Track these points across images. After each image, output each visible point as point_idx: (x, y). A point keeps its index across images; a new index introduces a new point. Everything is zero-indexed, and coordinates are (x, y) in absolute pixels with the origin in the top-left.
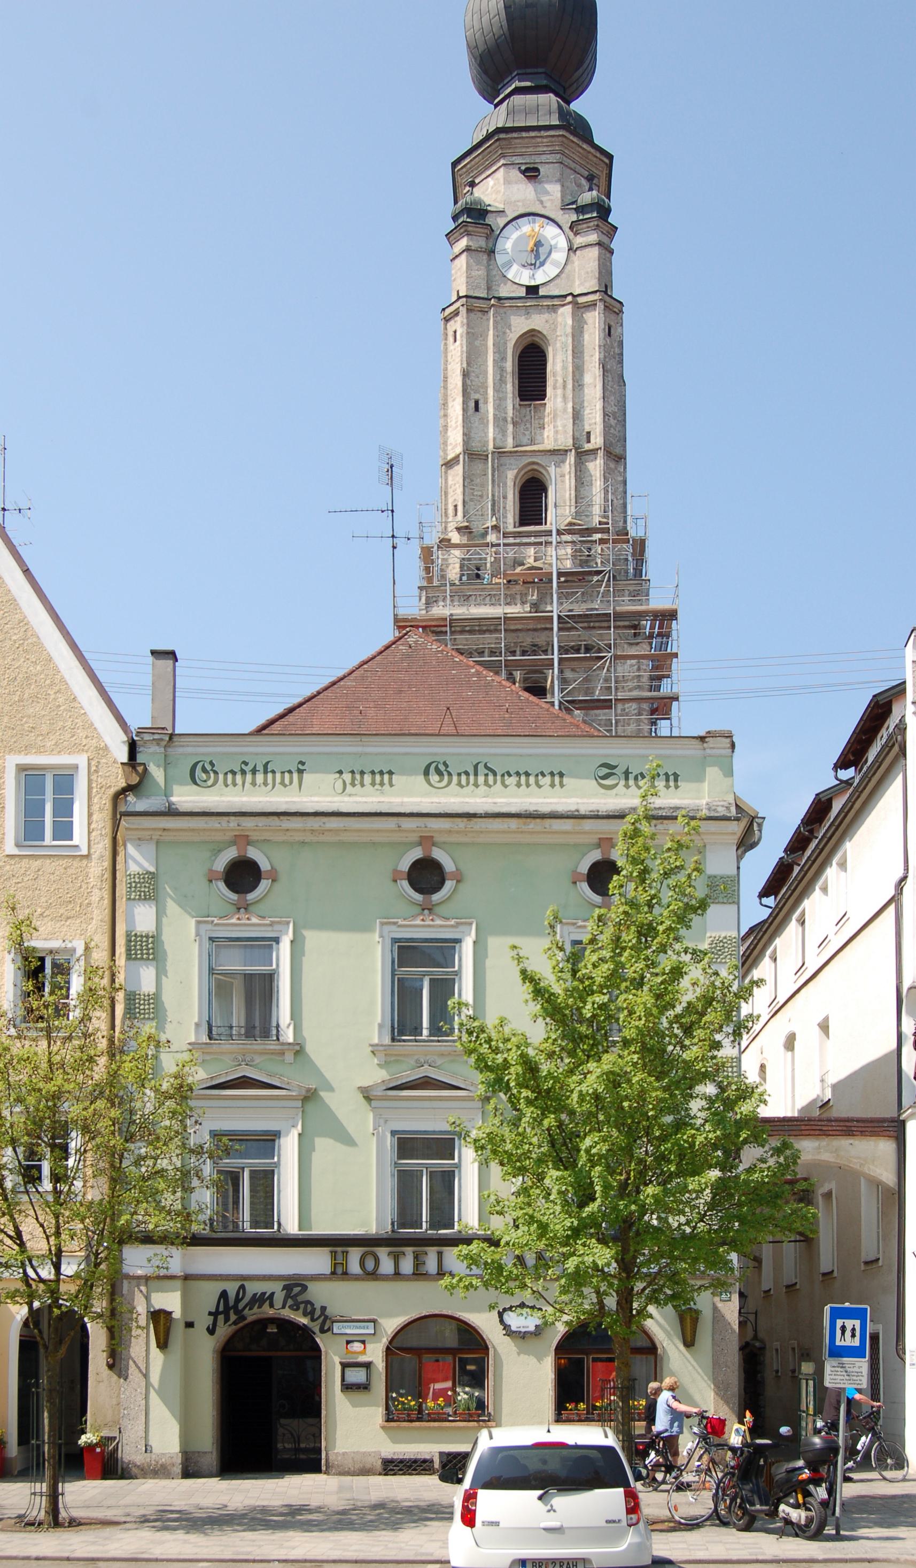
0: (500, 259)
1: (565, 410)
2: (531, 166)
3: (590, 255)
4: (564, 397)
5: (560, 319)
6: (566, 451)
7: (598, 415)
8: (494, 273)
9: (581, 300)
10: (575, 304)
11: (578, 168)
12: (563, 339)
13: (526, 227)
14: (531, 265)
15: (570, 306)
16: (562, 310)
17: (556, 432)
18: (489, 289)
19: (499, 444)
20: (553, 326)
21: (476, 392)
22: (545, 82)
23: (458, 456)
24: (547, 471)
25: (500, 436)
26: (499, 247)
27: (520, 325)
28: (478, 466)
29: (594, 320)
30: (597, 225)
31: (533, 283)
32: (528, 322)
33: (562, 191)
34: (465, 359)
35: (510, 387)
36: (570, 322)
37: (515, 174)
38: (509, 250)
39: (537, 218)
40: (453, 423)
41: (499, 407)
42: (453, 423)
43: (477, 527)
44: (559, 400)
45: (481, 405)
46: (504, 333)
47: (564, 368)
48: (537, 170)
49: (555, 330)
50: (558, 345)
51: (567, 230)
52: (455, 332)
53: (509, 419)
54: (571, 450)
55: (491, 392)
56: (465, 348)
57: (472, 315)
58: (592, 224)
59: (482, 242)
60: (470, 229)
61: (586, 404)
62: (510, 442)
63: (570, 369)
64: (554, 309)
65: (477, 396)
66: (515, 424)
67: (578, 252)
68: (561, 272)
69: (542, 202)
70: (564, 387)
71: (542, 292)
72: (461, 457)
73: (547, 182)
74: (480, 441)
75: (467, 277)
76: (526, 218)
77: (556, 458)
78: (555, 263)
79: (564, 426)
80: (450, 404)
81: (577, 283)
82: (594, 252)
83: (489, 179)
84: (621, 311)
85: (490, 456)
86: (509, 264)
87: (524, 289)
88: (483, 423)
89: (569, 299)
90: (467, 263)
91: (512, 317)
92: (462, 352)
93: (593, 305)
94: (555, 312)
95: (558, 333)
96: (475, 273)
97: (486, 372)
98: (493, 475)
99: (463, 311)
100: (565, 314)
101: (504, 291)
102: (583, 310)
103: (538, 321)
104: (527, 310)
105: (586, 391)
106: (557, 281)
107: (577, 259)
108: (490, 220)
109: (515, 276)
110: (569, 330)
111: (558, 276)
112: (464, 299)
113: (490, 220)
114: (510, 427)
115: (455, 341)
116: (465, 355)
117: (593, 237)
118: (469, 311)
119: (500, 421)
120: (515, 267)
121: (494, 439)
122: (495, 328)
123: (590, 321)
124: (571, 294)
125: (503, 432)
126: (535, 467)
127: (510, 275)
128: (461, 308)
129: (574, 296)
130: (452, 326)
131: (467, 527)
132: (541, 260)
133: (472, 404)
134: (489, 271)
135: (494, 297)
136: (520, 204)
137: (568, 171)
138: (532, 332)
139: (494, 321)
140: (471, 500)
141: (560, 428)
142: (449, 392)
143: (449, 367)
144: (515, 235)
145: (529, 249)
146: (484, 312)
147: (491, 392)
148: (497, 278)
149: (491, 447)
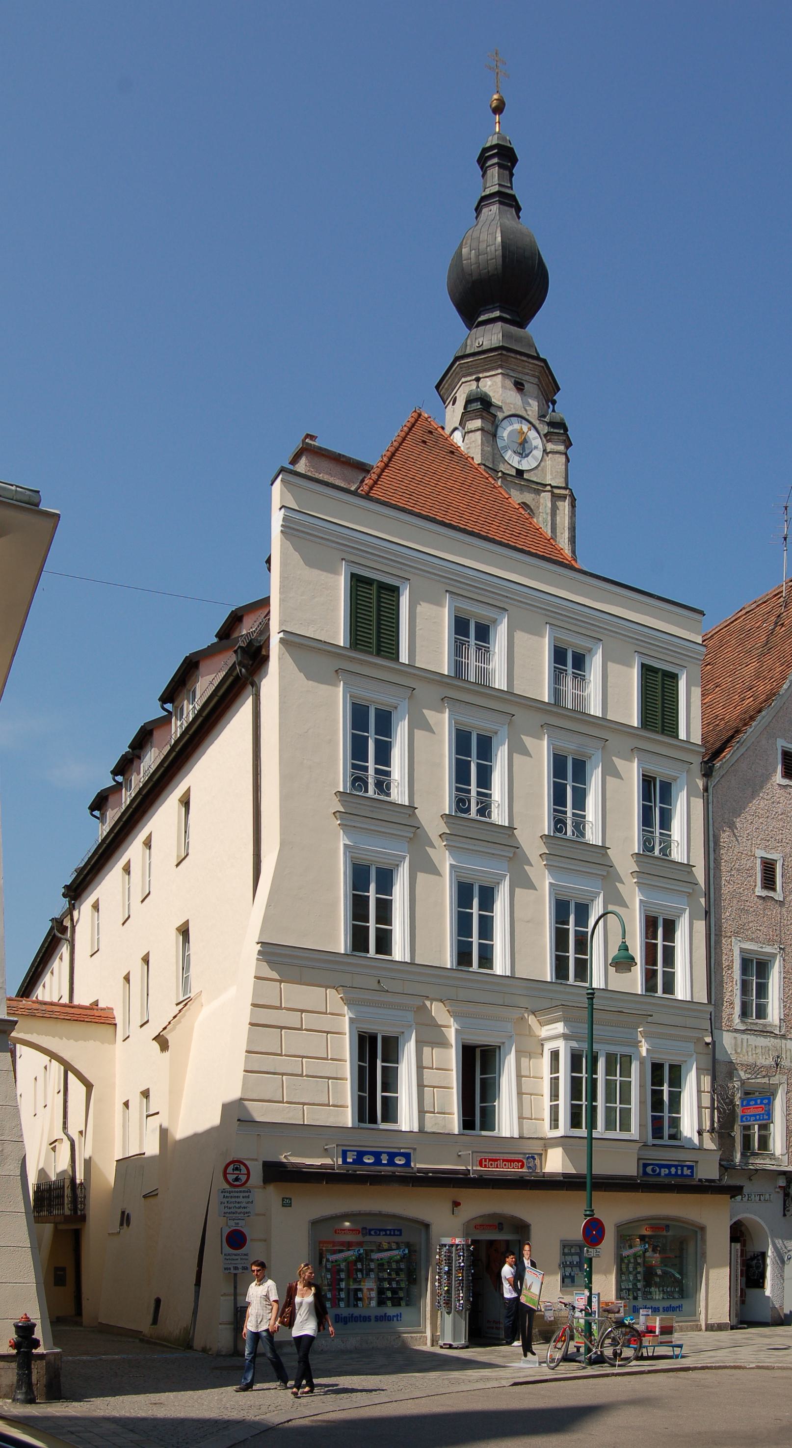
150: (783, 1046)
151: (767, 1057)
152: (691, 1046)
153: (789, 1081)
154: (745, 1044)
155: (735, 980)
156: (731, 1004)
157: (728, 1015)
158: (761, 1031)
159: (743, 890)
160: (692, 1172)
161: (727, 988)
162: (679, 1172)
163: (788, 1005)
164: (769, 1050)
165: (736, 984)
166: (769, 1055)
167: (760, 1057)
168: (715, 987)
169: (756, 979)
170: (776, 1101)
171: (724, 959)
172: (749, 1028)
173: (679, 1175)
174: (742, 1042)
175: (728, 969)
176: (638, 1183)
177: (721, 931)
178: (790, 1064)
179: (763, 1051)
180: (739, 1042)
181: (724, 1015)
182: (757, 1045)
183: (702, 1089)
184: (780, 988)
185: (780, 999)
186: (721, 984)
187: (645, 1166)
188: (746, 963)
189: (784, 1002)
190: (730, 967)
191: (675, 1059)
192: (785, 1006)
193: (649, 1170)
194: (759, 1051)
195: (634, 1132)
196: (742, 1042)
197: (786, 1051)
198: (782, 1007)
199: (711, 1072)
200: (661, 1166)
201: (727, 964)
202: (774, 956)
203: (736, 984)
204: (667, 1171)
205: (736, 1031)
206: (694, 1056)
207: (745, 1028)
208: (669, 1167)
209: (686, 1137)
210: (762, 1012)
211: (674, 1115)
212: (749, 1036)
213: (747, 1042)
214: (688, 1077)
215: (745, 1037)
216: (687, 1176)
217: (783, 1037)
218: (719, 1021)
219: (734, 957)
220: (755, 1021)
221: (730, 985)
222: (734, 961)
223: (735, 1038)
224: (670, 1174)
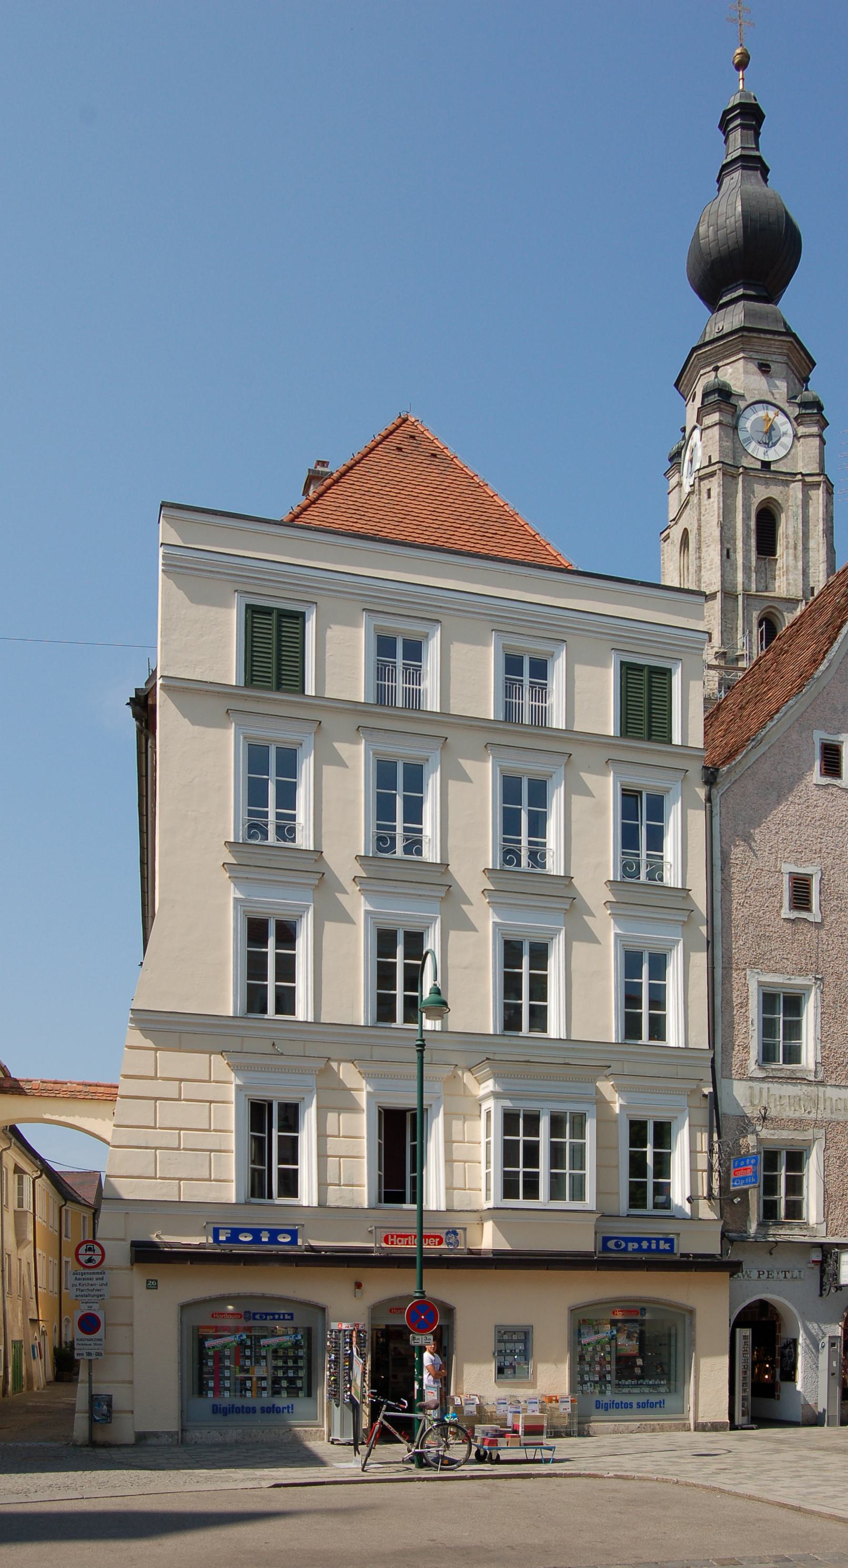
0: (742, 435)
1: (796, 567)
2: (765, 362)
3: (813, 443)
4: (795, 557)
5: (791, 492)
6: (798, 601)
7: (821, 574)
8: (737, 446)
9: (808, 479)
10: (803, 481)
11: (795, 371)
12: (794, 509)
13: (761, 412)
14: (765, 443)
15: (801, 483)
16: (792, 485)
17: (789, 584)
18: (734, 458)
19: (746, 588)
20: (786, 497)
21: (728, 542)
22: (765, 294)
23: (716, 593)
24: (783, 615)
25: (746, 581)
26: (741, 423)
27: (761, 492)
28: (730, 603)
29: (818, 496)
30: (819, 420)
31: (766, 459)
32: (768, 490)
33: (788, 387)
34: (721, 514)
35: (753, 542)
36: (800, 496)
37: (753, 367)
38: (749, 429)
39: (770, 407)
40: (707, 565)
41: (746, 557)
42: (707, 565)
43: (731, 655)
44: (791, 558)
45: (731, 554)
46: (750, 497)
47: (795, 533)
48: (769, 366)
49: (787, 500)
50: (790, 513)
51: (792, 420)
52: (709, 490)
53: (753, 568)
54: (802, 600)
55: (739, 544)
56: (721, 505)
57: (725, 478)
58: (814, 418)
59: (728, 419)
60: (722, 406)
61: (811, 564)
62: (753, 586)
63: (801, 534)
64: (786, 483)
65: (729, 546)
66: (756, 573)
67: (801, 440)
68: (788, 454)
69: (773, 394)
70: (795, 548)
71: (773, 468)
72: (719, 595)
73: (778, 378)
74: (730, 583)
75: (720, 446)
76: (761, 405)
77: (789, 605)
78: (784, 446)
79: (795, 580)
80: (704, 549)
81: (800, 464)
82: (816, 441)
83: (728, 367)
84: (833, 493)
85: (740, 598)
86: (749, 440)
87: (760, 463)
88: (732, 569)
89: (799, 477)
90: (720, 434)
91: (755, 485)
92: (719, 508)
93: (816, 485)
94: (788, 486)
95: (790, 504)
96: (725, 444)
97: (735, 527)
98: (743, 613)
99: (719, 474)
100: (796, 489)
101: (746, 462)
102: (808, 488)
103: (774, 492)
104: (767, 482)
105: (811, 554)
106: (785, 460)
107: (800, 446)
108: (733, 401)
109: (754, 450)
110: (800, 503)
111: (785, 456)
112: (721, 465)
113: (733, 401)
114: (754, 575)
115: (709, 497)
116: (721, 511)
117: (815, 430)
118: (724, 474)
119: (747, 569)
120: (753, 444)
121: (743, 583)
122: (743, 492)
123: (814, 497)
124: (801, 473)
125: (749, 578)
126: (772, 610)
127: (749, 451)
128: (718, 471)
129: (803, 475)
130: (705, 485)
131: (724, 653)
132: (774, 441)
133: (725, 552)
134: (734, 443)
135: (742, 466)
136: (756, 392)
137: (790, 372)
138: (770, 500)
139: (743, 486)
140: (725, 631)
141: (791, 581)
142: (703, 539)
143: (703, 518)
144: (753, 417)
145: (765, 430)
146: (734, 477)
147: (739, 544)
148: (739, 450)
149: (740, 588)
150: (821, 1095)
151: (797, 1108)
152: (684, 1100)
153: (829, 1136)
154: (765, 1094)
155: (750, 1019)
156: (746, 1047)
157: (742, 1061)
158: (789, 1078)
159: (764, 913)
160: (672, 1247)
161: (739, 1029)
162: (654, 1246)
163: (829, 1045)
164: (800, 1100)
165: (752, 1024)
166: (800, 1106)
167: (787, 1109)
168: (723, 1030)
169: (784, 1016)
170: (811, 1159)
171: (735, 996)
172: (771, 1075)
173: (653, 1250)
174: (761, 1092)
175: (741, 1007)
176: (596, 1260)
177: (731, 963)
178: (830, 1115)
179: (792, 1101)
180: (757, 1092)
181: (736, 1061)
182: (782, 1094)
183: (699, 1149)
184: (816, 1026)
185: (816, 1039)
186: (731, 1025)
187: (606, 1240)
188: (769, 1000)
189: (822, 1042)
190: (744, 1004)
191: (662, 1116)
192: (823, 1047)
193: (611, 1244)
194: (785, 1101)
195: (590, 1201)
196: (761, 1092)
197: (825, 1100)
198: (819, 1047)
199: (708, 1129)
200: (627, 1240)
201: (739, 1001)
202: (808, 988)
203: (752, 1024)
204: (636, 1246)
205: (752, 1079)
206: (687, 1112)
207: (764, 1075)
208: (639, 1241)
209: (677, 1205)
210: (792, 1055)
211: (661, 1180)
212: (770, 1085)
213: (769, 1091)
214: (679, 1136)
215: (765, 1086)
216: (664, 1251)
217: (821, 1083)
218: (728, 1069)
219: (750, 993)
220: (781, 1067)
221: (744, 1025)
222: (750, 997)
223: (751, 1087)
224: (640, 1250)
